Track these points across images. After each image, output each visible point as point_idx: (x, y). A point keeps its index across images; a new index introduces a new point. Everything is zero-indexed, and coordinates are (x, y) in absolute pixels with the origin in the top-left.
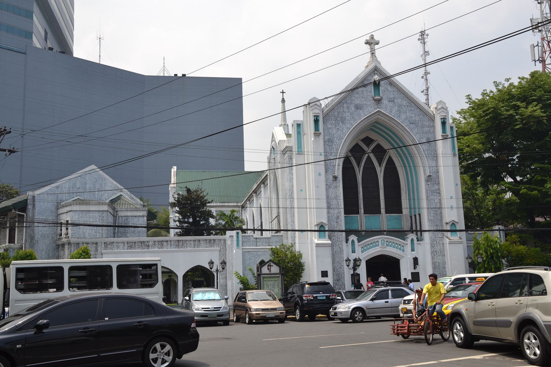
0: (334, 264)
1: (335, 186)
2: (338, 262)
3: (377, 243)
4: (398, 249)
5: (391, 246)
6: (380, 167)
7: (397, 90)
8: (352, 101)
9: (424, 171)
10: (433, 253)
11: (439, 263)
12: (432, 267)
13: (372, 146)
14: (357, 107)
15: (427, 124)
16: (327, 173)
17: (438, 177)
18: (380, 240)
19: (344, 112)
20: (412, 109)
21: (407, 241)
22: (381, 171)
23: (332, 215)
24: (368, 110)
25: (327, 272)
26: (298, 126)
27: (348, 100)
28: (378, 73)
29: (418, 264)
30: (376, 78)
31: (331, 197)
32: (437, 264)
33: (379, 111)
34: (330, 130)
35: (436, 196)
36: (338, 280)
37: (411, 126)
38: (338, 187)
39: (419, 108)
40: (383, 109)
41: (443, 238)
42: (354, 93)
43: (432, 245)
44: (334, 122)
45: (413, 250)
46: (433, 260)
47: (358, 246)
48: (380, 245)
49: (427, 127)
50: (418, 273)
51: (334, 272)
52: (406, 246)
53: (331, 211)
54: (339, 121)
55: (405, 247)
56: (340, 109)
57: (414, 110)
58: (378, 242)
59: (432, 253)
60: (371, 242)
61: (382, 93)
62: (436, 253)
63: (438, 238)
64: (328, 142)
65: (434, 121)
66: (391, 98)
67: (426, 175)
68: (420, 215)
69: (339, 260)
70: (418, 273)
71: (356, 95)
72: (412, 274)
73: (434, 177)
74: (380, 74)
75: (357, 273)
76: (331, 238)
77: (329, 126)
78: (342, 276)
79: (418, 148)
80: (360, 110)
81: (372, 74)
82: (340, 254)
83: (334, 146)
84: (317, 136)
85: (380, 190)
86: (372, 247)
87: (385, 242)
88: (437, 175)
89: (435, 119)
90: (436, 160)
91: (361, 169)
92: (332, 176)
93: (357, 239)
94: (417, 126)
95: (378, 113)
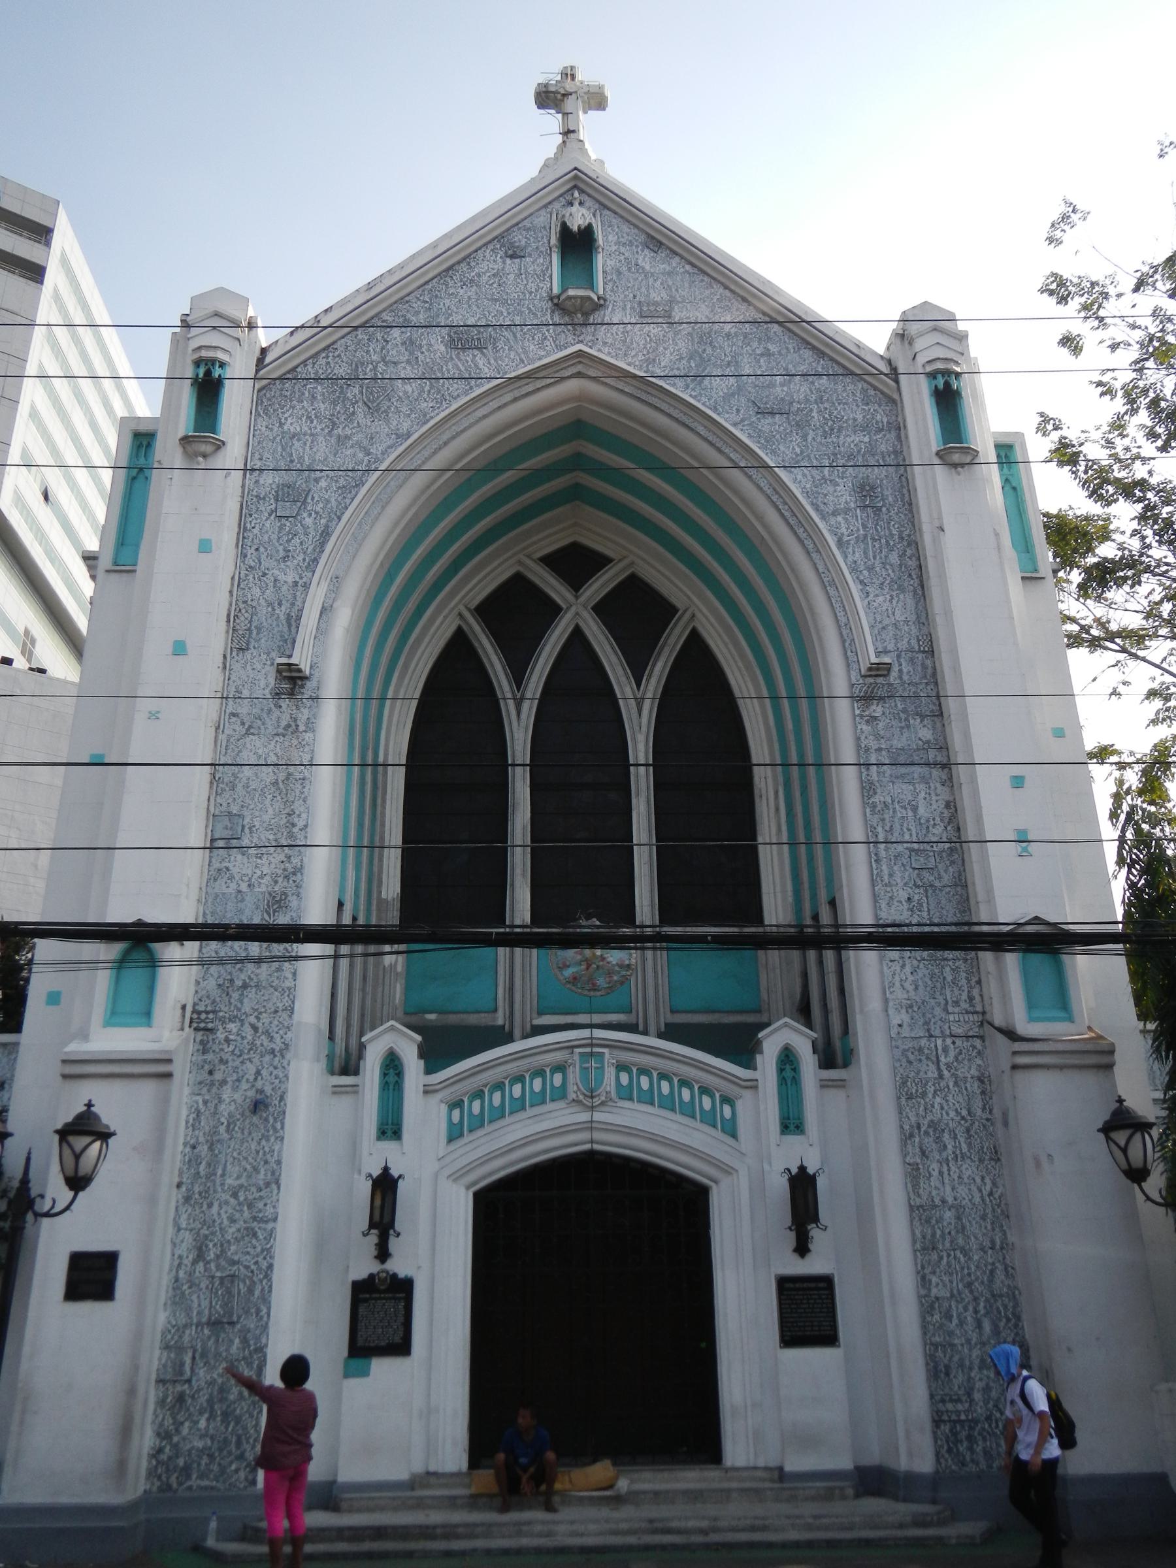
0: (210, 1205)
1: (283, 723)
2: (235, 1195)
3: (558, 1079)
4: (693, 1117)
5: (648, 1098)
6: (638, 686)
7: (688, 267)
8: (438, 316)
9: (848, 646)
10: (917, 1140)
11: (959, 1210)
12: (914, 1242)
13: (599, 586)
14: (460, 339)
15: (860, 417)
16: (248, 655)
17: (933, 677)
18: (576, 1058)
19: (386, 363)
20: (773, 348)
21: (755, 1069)
23: (244, 887)
24: (525, 352)
25: (109, 1260)
26: (139, 446)
27: (417, 313)
28: (589, 202)
29: (815, 1219)
30: (578, 217)
31: (253, 785)
32: (948, 1215)
33: (580, 353)
34: (297, 444)
35: (924, 780)
36: (216, 1324)
37: (766, 424)
38: (302, 728)
39: (808, 343)
40: (606, 350)
41: (982, 1038)
42: (451, 284)
43: (904, 1083)
44: (322, 406)
45: (791, 1124)
46: (916, 1186)
47: (426, 1092)
48: (571, 1089)
49: (855, 432)
50: (825, 1284)
51: (200, 1267)
52: (747, 1094)
53: (238, 863)
54: (353, 404)
55: (739, 1104)
56: (368, 352)
57: (784, 351)
58: (561, 1068)
59: (906, 1138)
60: (512, 1068)
61: (605, 283)
62: (938, 1140)
63: (944, 1037)
64: (277, 500)
65: (894, 401)
66: (656, 304)
67: (855, 666)
68: (832, 903)
69: (243, 1181)
70: (825, 1284)
71: (462, 292)
72: (785, 1285)
73: (906, 678)
74: (601, 203)
75: (395, 1276)
76: (211, 1030)
77: (292, 425)
78: (251, 1291)
79: (806, 530)
80: (476, 352)
81: (557, 206)
82: (257, 1135)
83: (309, 521)
84: (201, 459)
85: (634, 801)
86: (520, 1105)
87: (610, 1073)
88: (924, 667)
89: (899, 389)
90: (915, 591)
91: (529, 695)
92: (272, 671)
93: (420, 1047)
94: (797, 424)
95: (580, 368)
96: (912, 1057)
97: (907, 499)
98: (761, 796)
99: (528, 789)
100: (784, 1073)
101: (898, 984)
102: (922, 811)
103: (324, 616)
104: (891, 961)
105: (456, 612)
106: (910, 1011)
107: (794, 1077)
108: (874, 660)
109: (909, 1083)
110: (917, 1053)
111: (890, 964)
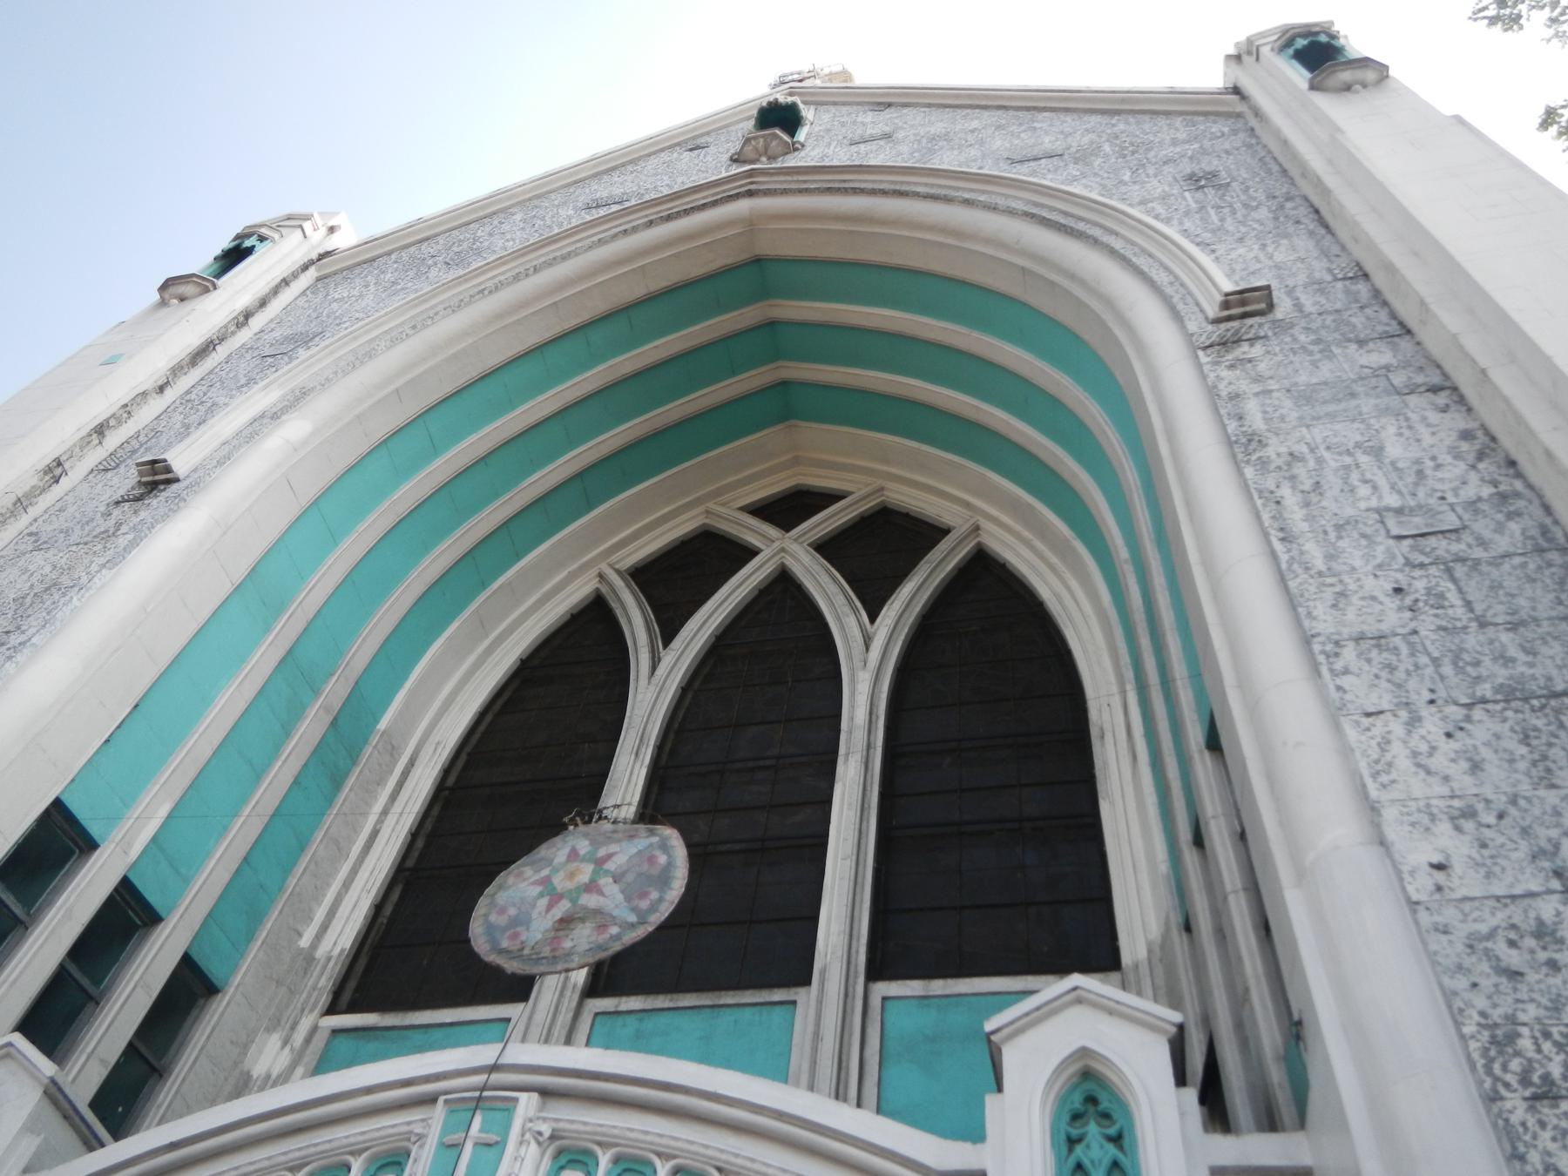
22: (867, 642)
43: (1502, 1039)
96: (1513, 958)
97: (1275, 168)
98: (1102, 737)
99: (644, 772)
100: (1079, 1150)
101: (1404, 763)
102: (1394, 450)
103: (256, 424)
104: (1368, 715)
105: (594, 572)
106: (1468, 825)
107: (1115, 1164)
108: (1228, 286)
109: (1525, 1044)
110: (1530, 942)
111: (1366, 721)
